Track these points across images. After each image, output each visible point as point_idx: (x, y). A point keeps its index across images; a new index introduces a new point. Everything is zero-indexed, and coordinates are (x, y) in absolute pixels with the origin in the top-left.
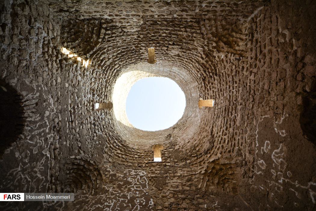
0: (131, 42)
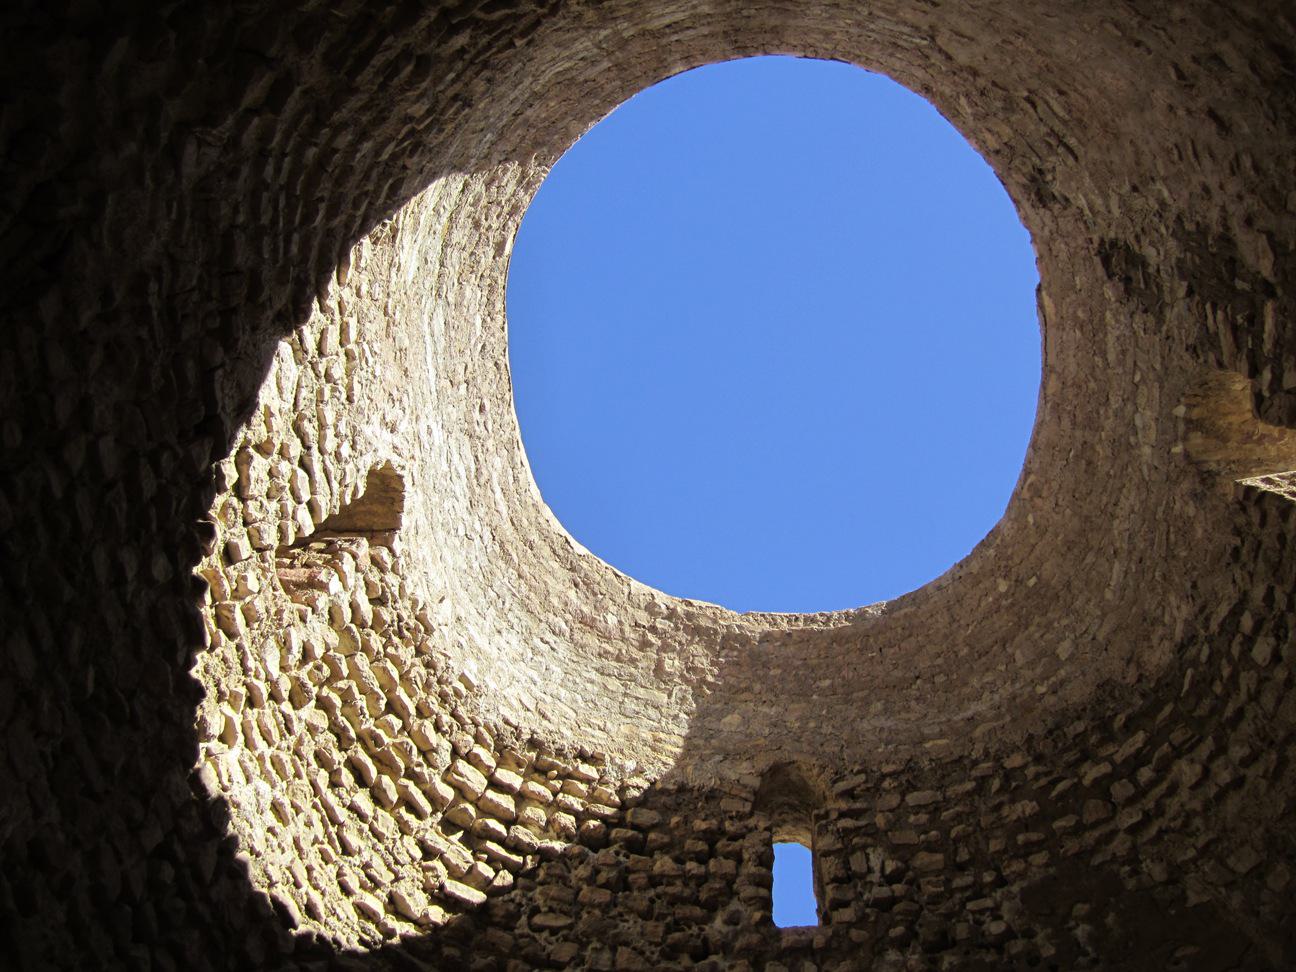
0: (276, 762)
